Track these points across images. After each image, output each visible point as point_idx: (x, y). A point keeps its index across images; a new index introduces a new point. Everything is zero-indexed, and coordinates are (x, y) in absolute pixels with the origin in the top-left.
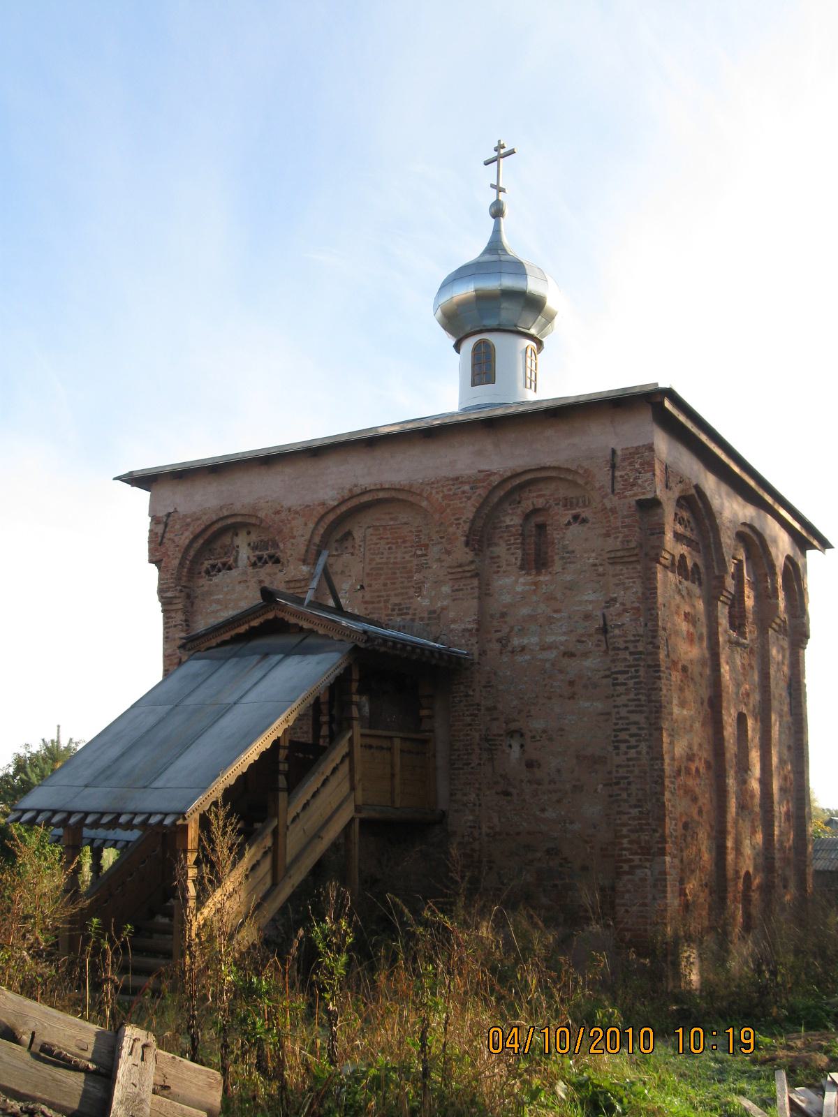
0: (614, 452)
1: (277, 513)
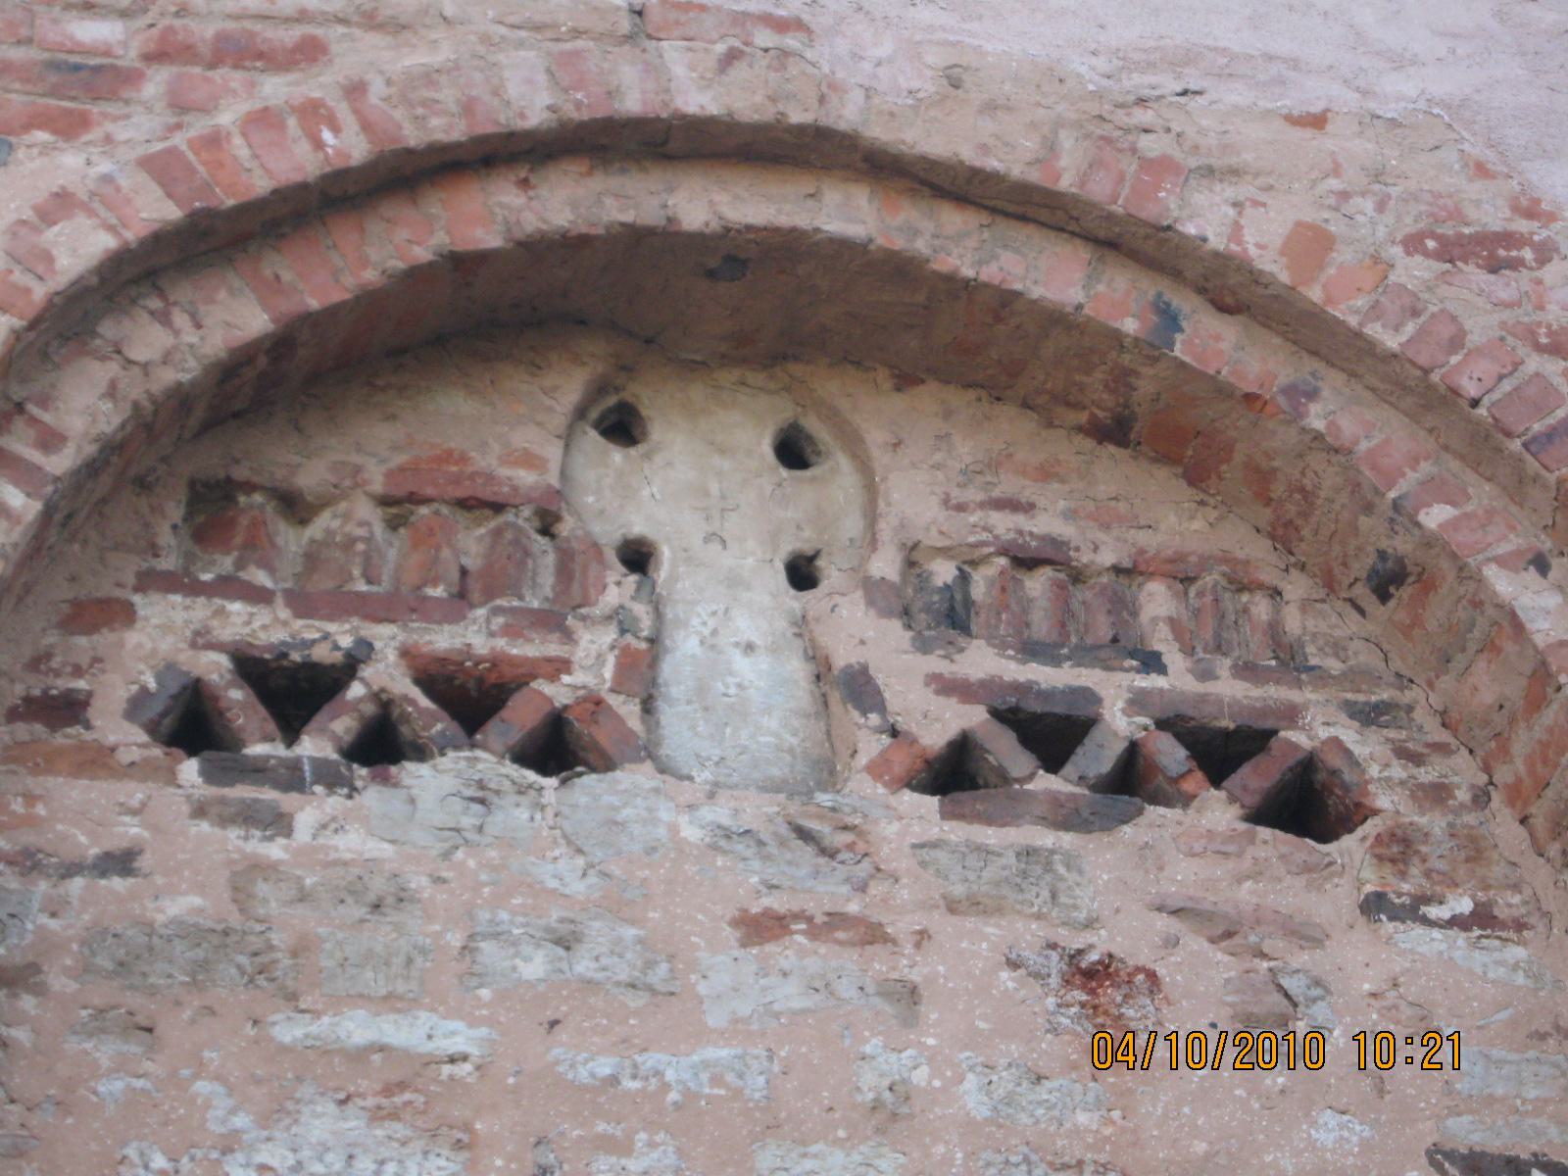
1: (1494, 252)
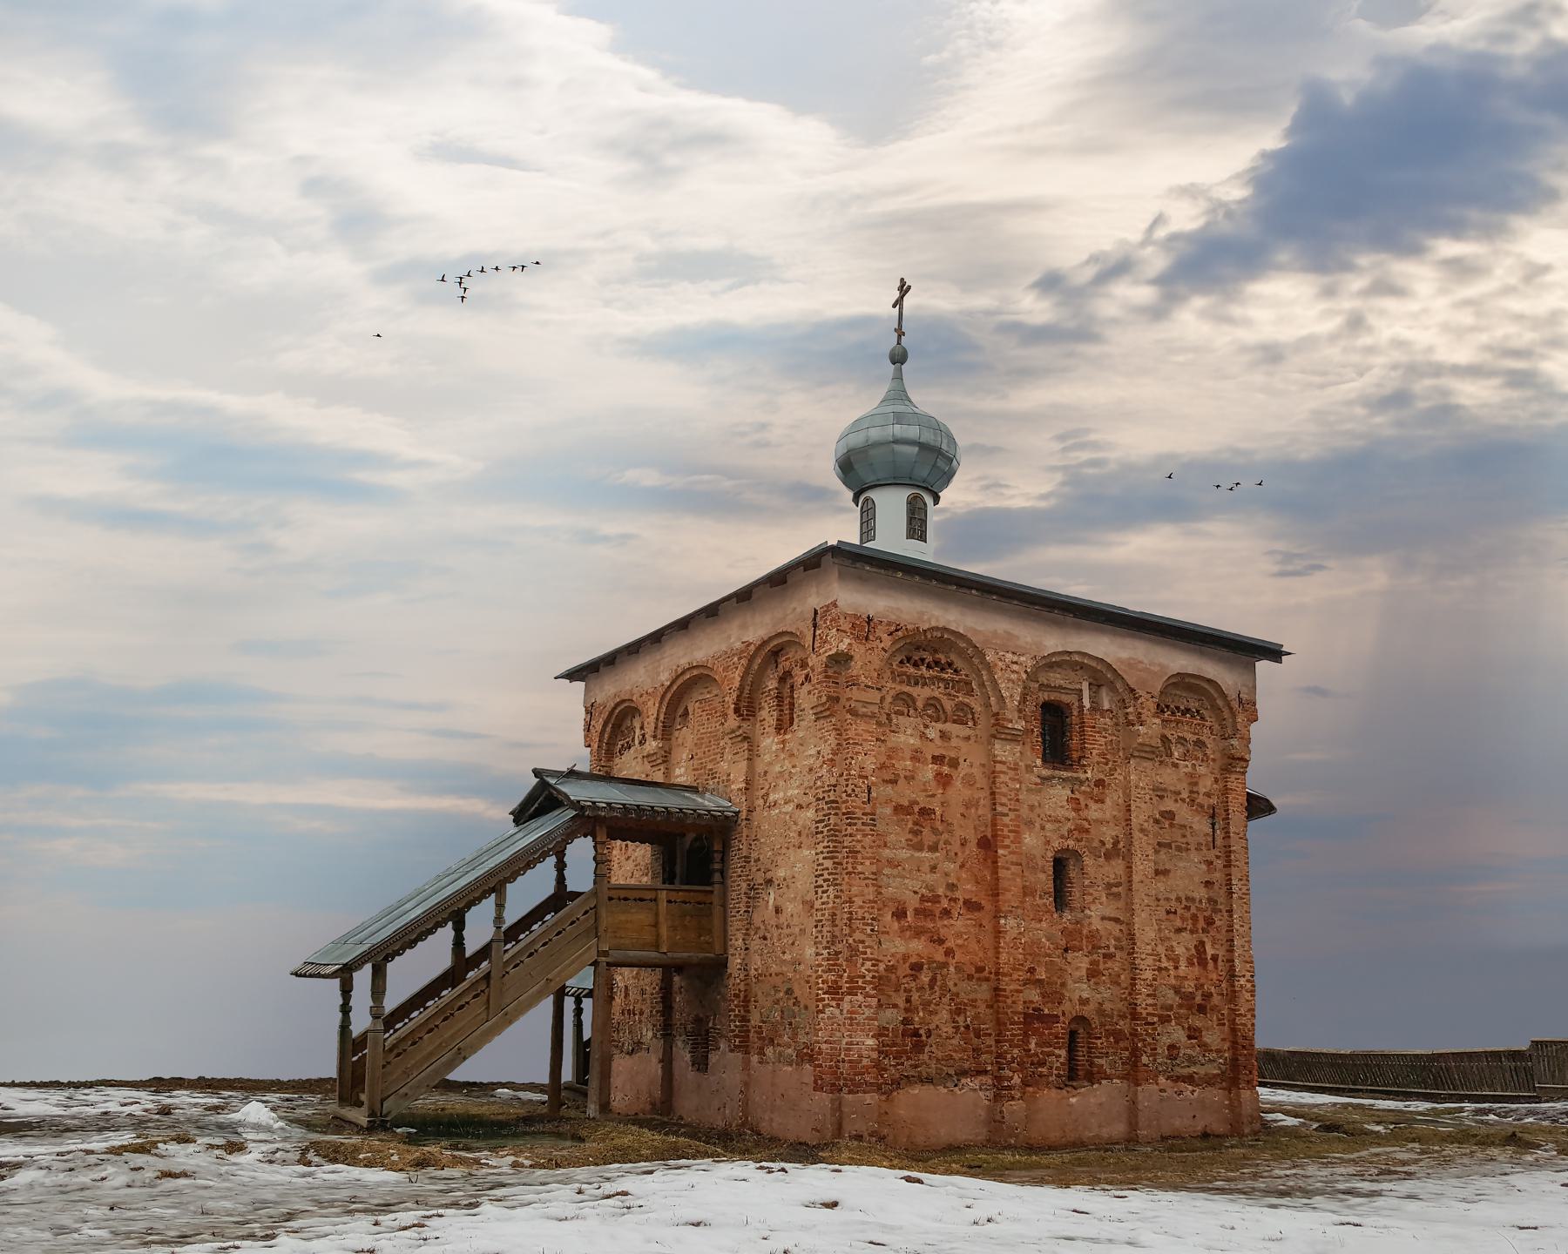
0: (816, 612)
